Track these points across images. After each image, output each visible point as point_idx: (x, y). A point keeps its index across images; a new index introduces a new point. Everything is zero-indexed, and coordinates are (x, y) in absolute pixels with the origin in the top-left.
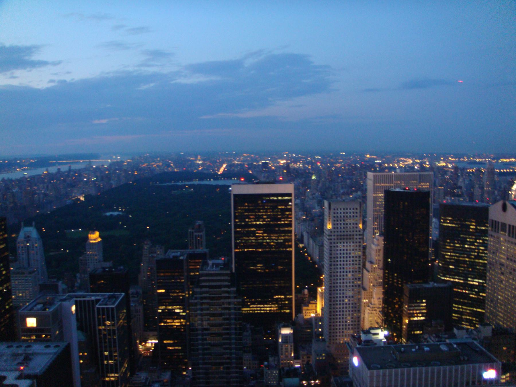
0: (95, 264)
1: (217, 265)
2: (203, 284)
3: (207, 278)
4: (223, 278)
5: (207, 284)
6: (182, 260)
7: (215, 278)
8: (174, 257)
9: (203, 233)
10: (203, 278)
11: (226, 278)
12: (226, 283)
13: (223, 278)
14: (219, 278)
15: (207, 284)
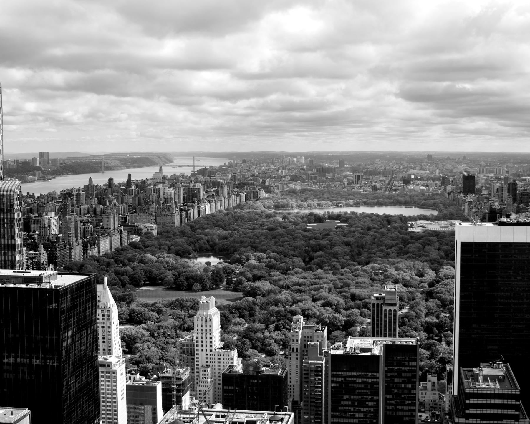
0: (208, 352)
1: (494, 378)
2: (471, 411)
3: (479, 401)
4: (505, 402)
5: (479, 411)
6: (378, 357)
7: (492, 401)
8: (363, 350)
9: (397, 308)
10: (472, 401)
11: (513, 402)
12: (513, 412)
13: (505, 402)
14: (500, 402)
15: (479, 411)
